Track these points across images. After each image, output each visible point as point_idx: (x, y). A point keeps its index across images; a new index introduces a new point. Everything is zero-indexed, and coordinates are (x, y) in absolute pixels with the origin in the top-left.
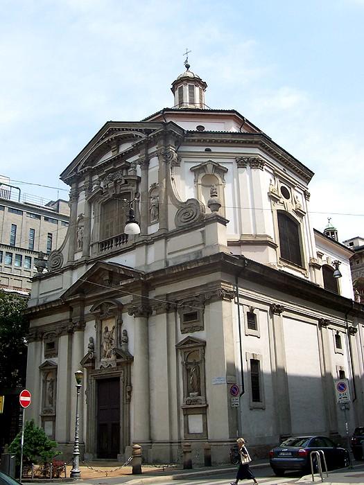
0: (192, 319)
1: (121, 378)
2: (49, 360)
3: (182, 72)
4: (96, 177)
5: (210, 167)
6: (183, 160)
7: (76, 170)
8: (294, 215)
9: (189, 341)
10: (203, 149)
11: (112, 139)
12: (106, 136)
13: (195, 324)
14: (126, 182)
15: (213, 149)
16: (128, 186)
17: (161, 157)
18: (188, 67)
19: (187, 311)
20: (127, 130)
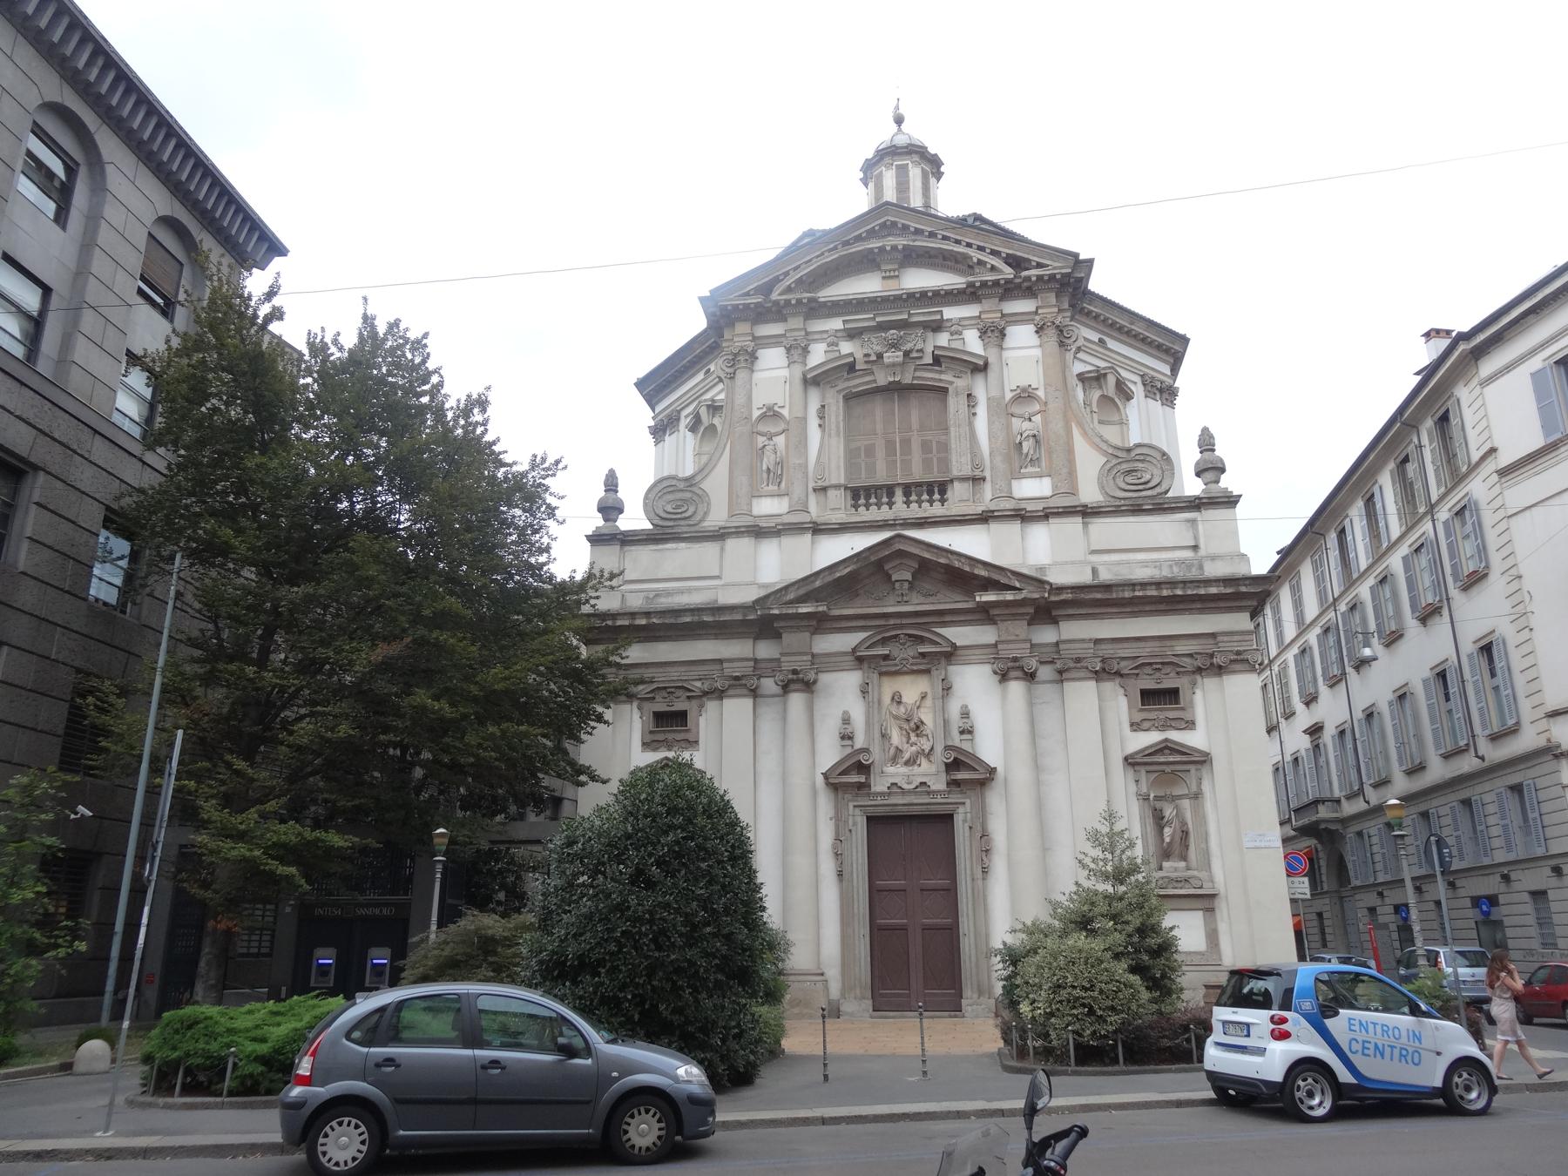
0: (1160, 700)
1: (959, 819)
3: (885, 133)
5: (1111, 380)
7: (767, 289)
9: (1166, 747)
10: (1095, 337)
11: (894, 248)
12: (872, 234)
13: (1171, 715)
14: (937, 360)
15: (1111, 344)
16: (941, 372)
17: (1051, 333)
18: (899, 120)
19: (1150, 685)
20: (945, 238)
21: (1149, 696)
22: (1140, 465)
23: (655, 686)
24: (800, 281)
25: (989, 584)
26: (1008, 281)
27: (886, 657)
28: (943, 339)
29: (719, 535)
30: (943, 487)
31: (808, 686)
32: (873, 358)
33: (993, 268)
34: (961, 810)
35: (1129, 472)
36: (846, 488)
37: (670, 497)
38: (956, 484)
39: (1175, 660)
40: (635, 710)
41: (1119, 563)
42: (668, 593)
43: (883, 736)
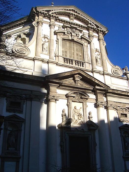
11: (74, 15)
14: (82, 38)
22: (117, 70)
23: (12, 94)
24: (55, 13)
25: (99, 85)
27: (74, 97)
29: (34, 60)
32: (69, 33)
33: (93, 25)
34: (90, 136)
35: (116, 70)
39: (126, 108)
40: (5, 100)
41: (117, 87)
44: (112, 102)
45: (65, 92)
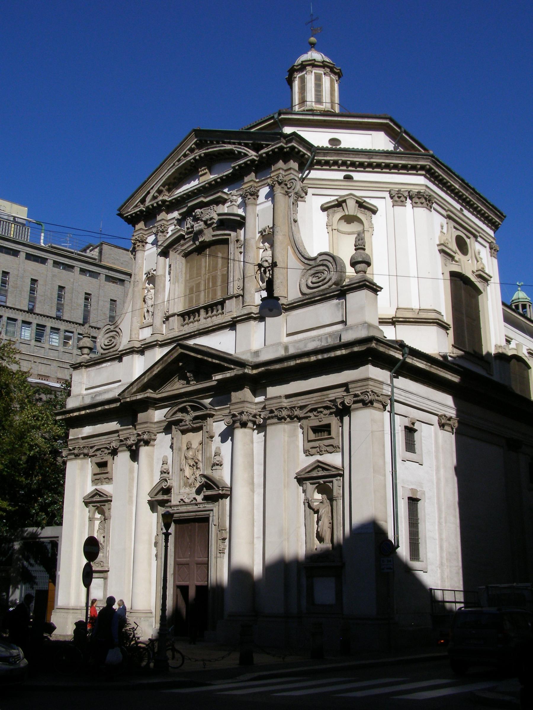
2: (99, 487)
4: (176, 214)
5: (351, 204)
6: (310, 191)
7: (143, 201)
8: (473, 279)
10: (340, 175)
15: (357, 176)
19: (315, 423)
21: (316, 430)
23: (95, 448)
24: (159, 192)
26: (253, 161)
27: (181, 421)
28: (224, 209)
30: (222, 303)
31: (147, 443)
36: (178, 315)
37: (108, 335)
38: (227, 301)
41: (300, 341)
42: (100, 393)
43: (181, 470)
44: (278, 401)
45: (158, 415)
